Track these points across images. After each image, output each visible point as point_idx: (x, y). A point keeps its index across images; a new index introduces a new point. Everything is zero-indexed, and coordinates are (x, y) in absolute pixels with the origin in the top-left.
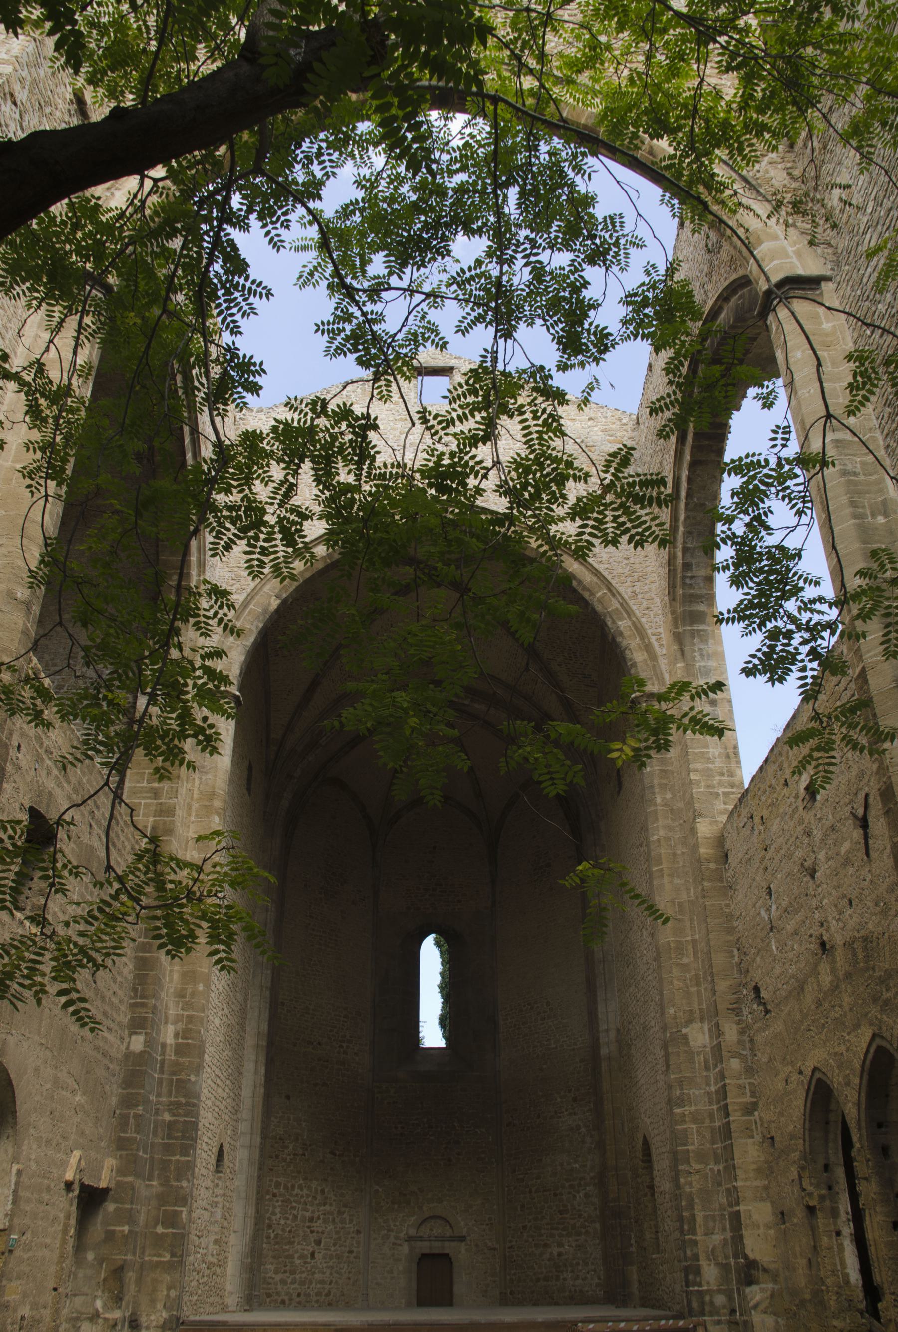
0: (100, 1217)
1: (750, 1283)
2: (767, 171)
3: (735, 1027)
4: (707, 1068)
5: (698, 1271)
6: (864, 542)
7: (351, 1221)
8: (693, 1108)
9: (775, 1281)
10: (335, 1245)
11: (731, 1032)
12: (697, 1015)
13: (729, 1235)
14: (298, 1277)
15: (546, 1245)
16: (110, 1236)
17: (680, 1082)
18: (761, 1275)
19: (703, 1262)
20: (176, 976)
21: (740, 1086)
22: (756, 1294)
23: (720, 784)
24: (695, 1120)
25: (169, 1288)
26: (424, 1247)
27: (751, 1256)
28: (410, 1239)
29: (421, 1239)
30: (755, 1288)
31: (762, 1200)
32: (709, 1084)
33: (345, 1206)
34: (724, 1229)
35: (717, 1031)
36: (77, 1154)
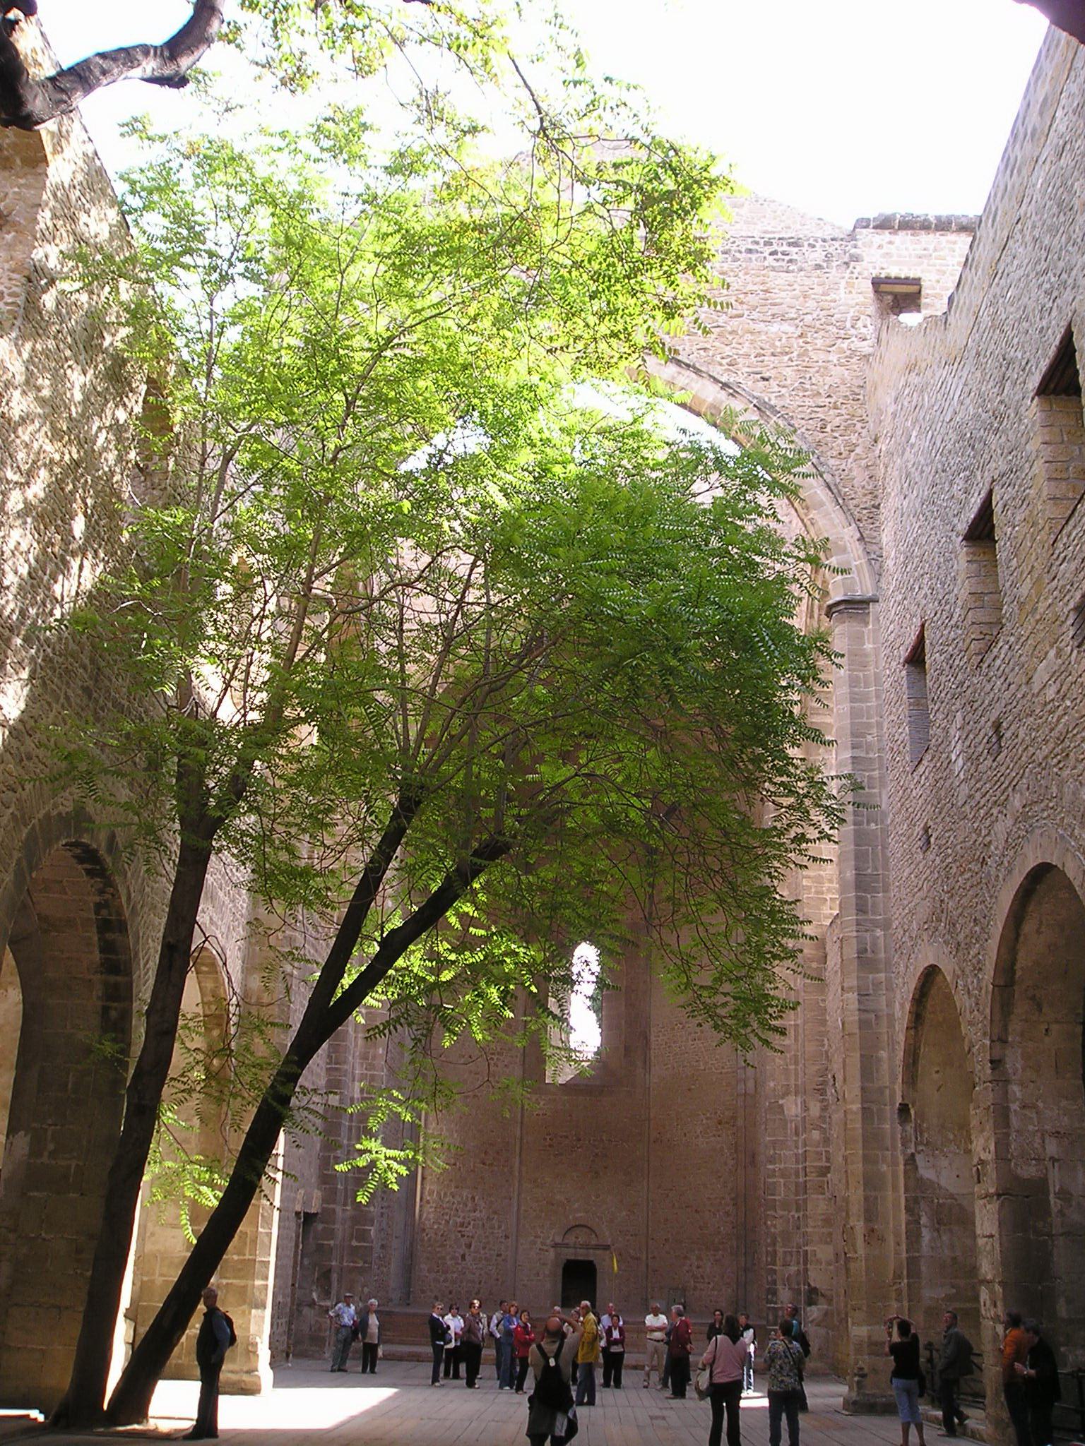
0: (312, 1235)
1: (810, 1304)
2: (851, 470)
3: (819, 1104)
4: (797, 1134)
5: (775, 1293)
6: (856, 845)
7: (500, 1227)
8: (782, 1166)
9: (830, 1304)
10: (484, 1248)
11: (815, 1109)
12: (793, 1089)
13: (802, 1267)
14: (449, 1276)
15: (686, 1258)
16: (320, 1248)
17: (774, 1142)
18: (821, 1300)
19: (779, 1287)
20: (360, 1042)
21: (817, 1153)
22: (814, 1312)
23: (829, 890)
24: (783, 1176)
25: (363, 1287)
26: (570, 1254)
27: (813, 1285)
28: (555, 1245)
29: (567, 1246)
30: (814, 1308)
31: (826, 1243)
32: (797, 1148)
33: (495, 1213)
34: (798, 1263)
35: (806, 1108)
36: (302, 1191)
